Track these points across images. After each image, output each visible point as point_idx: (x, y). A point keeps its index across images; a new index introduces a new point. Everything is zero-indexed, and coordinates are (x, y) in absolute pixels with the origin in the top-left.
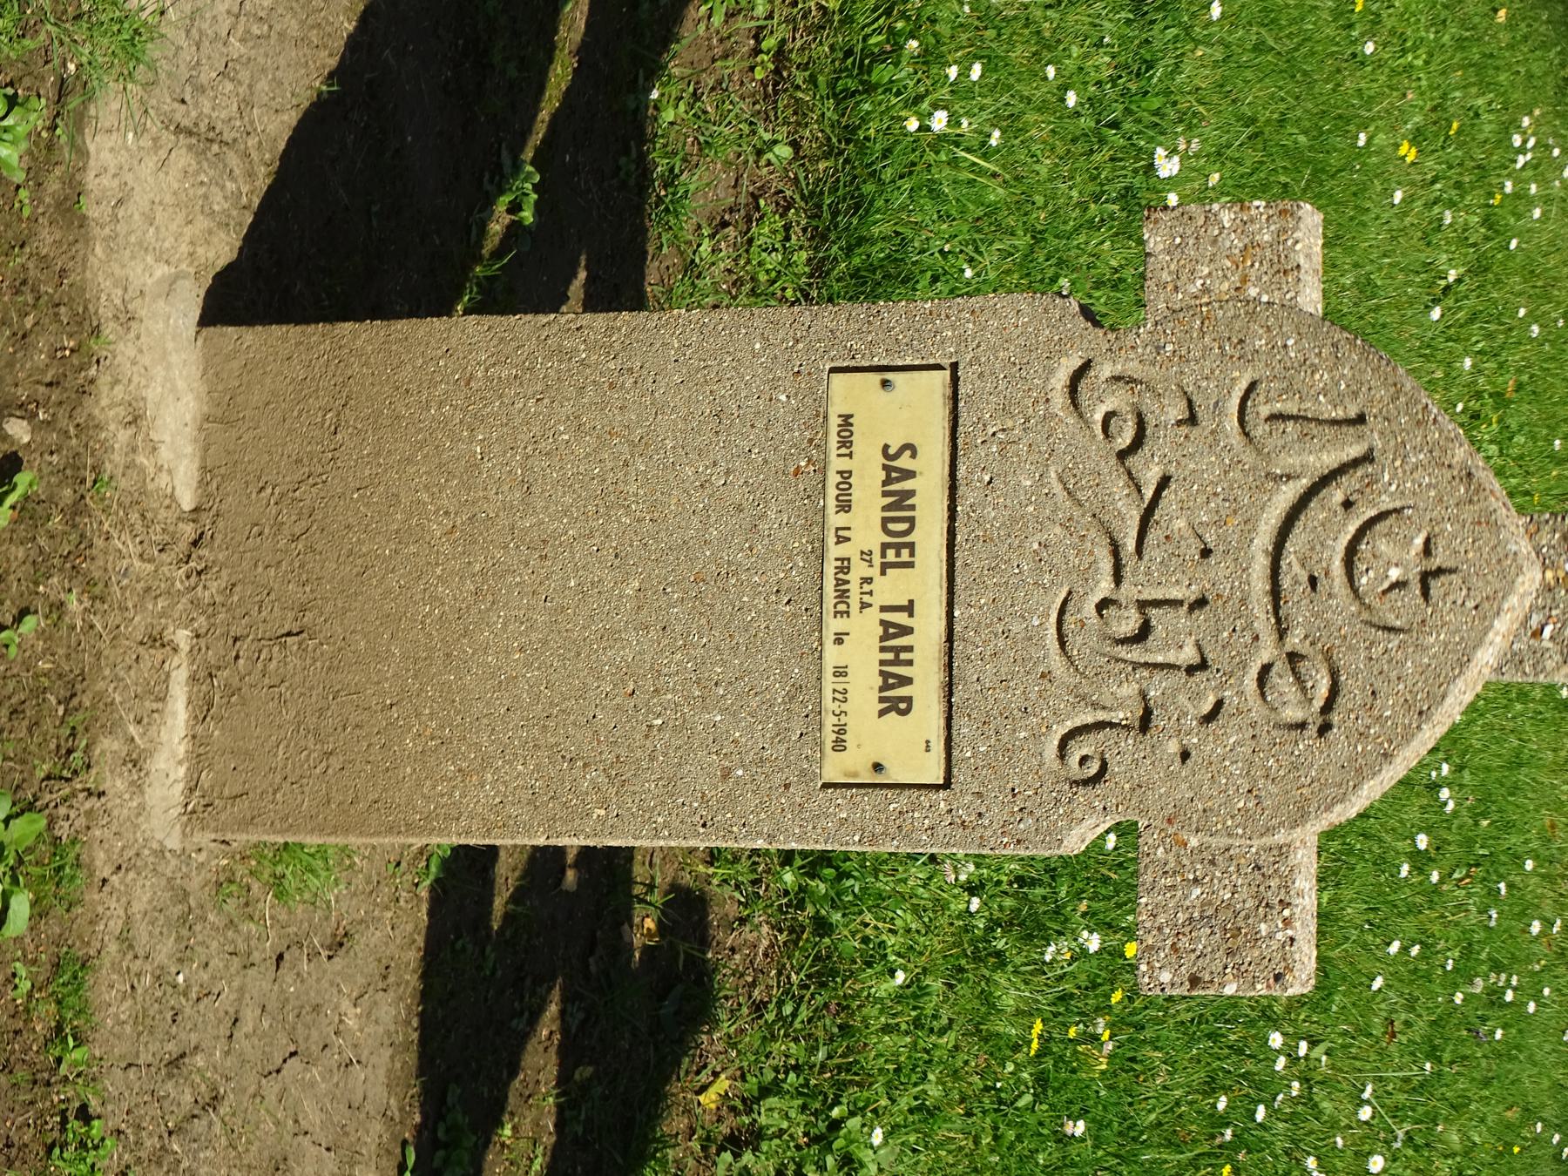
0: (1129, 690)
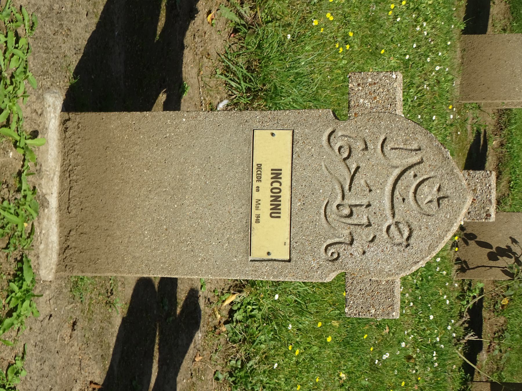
0: (346, 232)
